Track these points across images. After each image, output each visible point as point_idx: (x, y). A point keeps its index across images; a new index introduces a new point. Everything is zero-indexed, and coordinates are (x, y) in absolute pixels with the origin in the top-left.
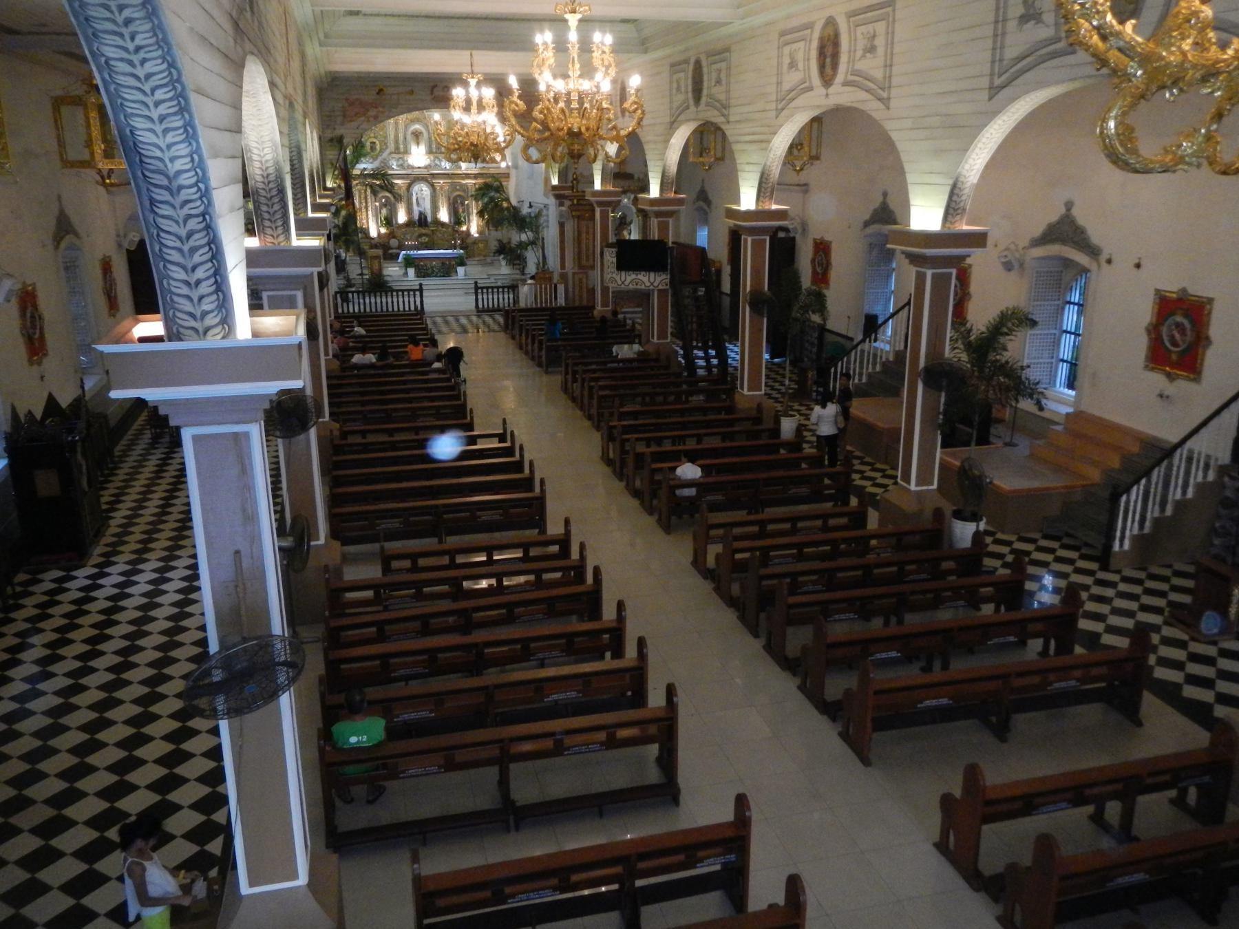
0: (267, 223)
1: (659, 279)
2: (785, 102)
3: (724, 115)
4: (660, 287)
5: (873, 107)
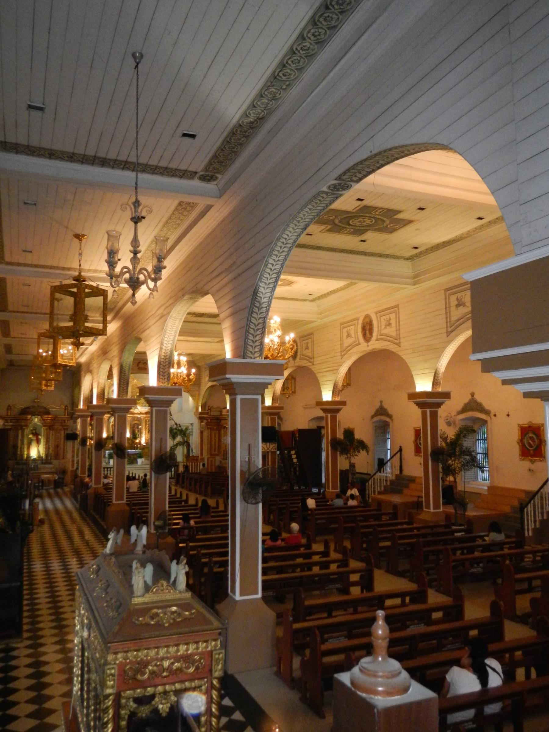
0: (161, 377)
1: (272, 446)
2: (345, 352)
3: (310, 362)
4: (272, 450)
5: (393, 348)
